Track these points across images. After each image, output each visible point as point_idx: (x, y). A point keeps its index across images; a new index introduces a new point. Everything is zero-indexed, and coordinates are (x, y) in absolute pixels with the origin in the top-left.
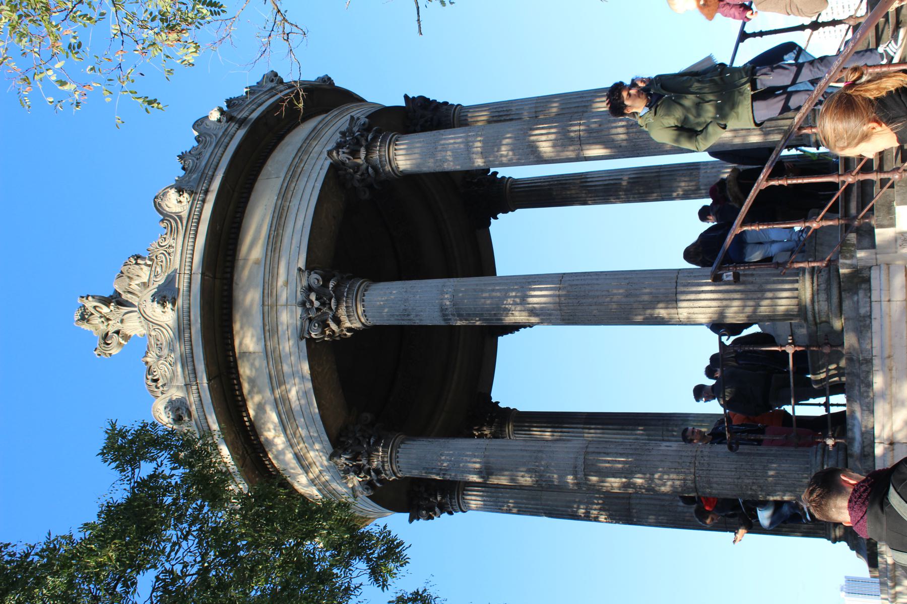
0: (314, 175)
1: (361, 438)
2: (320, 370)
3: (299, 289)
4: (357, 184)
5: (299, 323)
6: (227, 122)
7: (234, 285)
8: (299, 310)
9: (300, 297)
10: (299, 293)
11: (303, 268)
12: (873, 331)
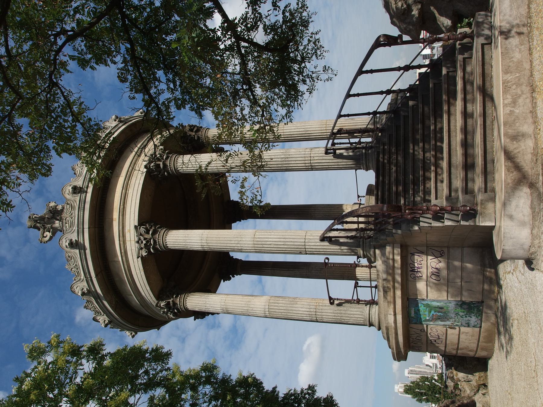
1: (169, 295)
3: (136, 235)
9: (137, 239)
10: (136, 237)
11: (137, 224)
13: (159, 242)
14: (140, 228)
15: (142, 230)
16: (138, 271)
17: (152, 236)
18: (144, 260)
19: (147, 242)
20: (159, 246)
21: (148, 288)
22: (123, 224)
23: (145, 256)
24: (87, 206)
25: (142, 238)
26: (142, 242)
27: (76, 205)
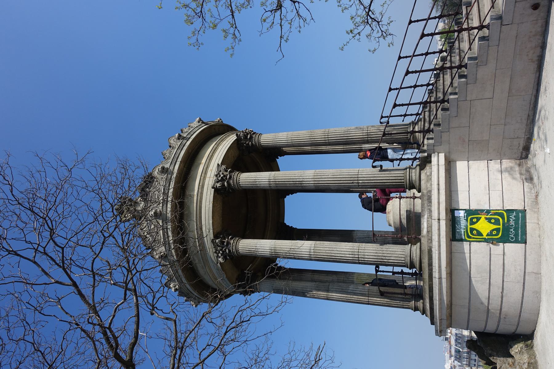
0: (230, 141)
2: (216, 205)
3: (216, 171)
4: (244, 148)
5: (213, 184)
6: (201, 123)
7: (191, 171)
8: (215, 178)
9: (216, 174)
10: (216, 172)
11: (220, 164)
12: (432, 180)
13: (233, 177)
14: (221, 166)
15: (224, 167)
16: (207, 204)
17: (229, 173)
18: (217, 191)
19: (224, 176)
20: (233, 181)
21: (211, 222)
22: (208, 165)
23: (219, 187)
24: (185, 148)
25: (221, 173)
26: (220, 176)
27: (176, 146)
